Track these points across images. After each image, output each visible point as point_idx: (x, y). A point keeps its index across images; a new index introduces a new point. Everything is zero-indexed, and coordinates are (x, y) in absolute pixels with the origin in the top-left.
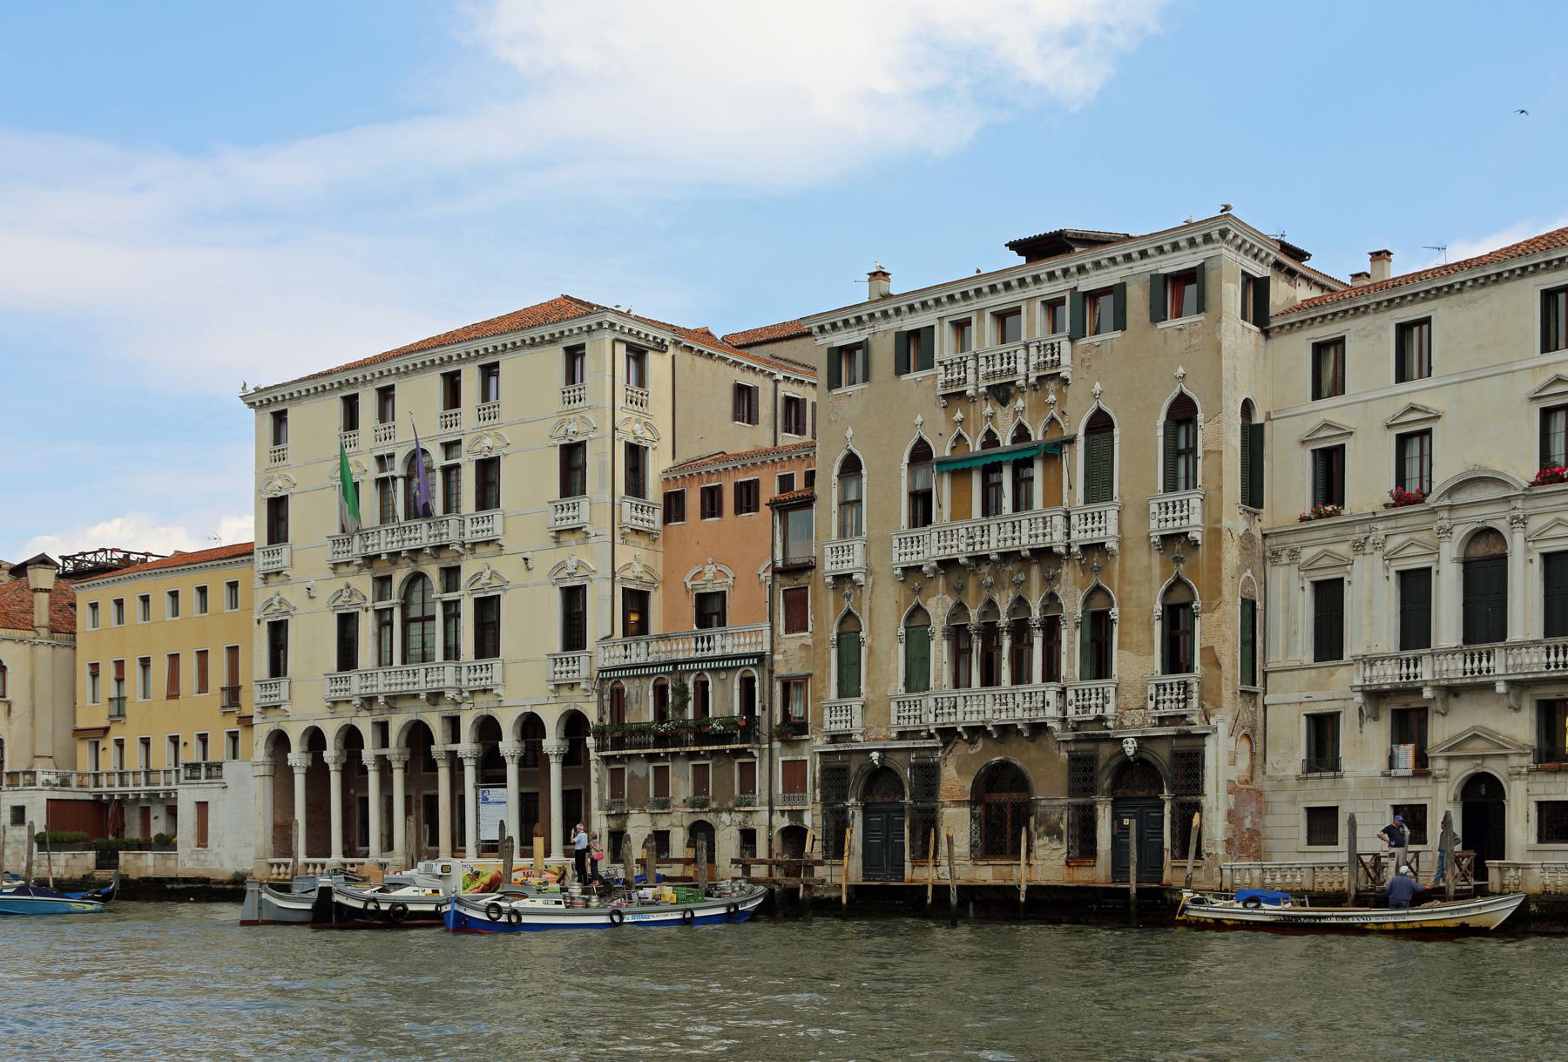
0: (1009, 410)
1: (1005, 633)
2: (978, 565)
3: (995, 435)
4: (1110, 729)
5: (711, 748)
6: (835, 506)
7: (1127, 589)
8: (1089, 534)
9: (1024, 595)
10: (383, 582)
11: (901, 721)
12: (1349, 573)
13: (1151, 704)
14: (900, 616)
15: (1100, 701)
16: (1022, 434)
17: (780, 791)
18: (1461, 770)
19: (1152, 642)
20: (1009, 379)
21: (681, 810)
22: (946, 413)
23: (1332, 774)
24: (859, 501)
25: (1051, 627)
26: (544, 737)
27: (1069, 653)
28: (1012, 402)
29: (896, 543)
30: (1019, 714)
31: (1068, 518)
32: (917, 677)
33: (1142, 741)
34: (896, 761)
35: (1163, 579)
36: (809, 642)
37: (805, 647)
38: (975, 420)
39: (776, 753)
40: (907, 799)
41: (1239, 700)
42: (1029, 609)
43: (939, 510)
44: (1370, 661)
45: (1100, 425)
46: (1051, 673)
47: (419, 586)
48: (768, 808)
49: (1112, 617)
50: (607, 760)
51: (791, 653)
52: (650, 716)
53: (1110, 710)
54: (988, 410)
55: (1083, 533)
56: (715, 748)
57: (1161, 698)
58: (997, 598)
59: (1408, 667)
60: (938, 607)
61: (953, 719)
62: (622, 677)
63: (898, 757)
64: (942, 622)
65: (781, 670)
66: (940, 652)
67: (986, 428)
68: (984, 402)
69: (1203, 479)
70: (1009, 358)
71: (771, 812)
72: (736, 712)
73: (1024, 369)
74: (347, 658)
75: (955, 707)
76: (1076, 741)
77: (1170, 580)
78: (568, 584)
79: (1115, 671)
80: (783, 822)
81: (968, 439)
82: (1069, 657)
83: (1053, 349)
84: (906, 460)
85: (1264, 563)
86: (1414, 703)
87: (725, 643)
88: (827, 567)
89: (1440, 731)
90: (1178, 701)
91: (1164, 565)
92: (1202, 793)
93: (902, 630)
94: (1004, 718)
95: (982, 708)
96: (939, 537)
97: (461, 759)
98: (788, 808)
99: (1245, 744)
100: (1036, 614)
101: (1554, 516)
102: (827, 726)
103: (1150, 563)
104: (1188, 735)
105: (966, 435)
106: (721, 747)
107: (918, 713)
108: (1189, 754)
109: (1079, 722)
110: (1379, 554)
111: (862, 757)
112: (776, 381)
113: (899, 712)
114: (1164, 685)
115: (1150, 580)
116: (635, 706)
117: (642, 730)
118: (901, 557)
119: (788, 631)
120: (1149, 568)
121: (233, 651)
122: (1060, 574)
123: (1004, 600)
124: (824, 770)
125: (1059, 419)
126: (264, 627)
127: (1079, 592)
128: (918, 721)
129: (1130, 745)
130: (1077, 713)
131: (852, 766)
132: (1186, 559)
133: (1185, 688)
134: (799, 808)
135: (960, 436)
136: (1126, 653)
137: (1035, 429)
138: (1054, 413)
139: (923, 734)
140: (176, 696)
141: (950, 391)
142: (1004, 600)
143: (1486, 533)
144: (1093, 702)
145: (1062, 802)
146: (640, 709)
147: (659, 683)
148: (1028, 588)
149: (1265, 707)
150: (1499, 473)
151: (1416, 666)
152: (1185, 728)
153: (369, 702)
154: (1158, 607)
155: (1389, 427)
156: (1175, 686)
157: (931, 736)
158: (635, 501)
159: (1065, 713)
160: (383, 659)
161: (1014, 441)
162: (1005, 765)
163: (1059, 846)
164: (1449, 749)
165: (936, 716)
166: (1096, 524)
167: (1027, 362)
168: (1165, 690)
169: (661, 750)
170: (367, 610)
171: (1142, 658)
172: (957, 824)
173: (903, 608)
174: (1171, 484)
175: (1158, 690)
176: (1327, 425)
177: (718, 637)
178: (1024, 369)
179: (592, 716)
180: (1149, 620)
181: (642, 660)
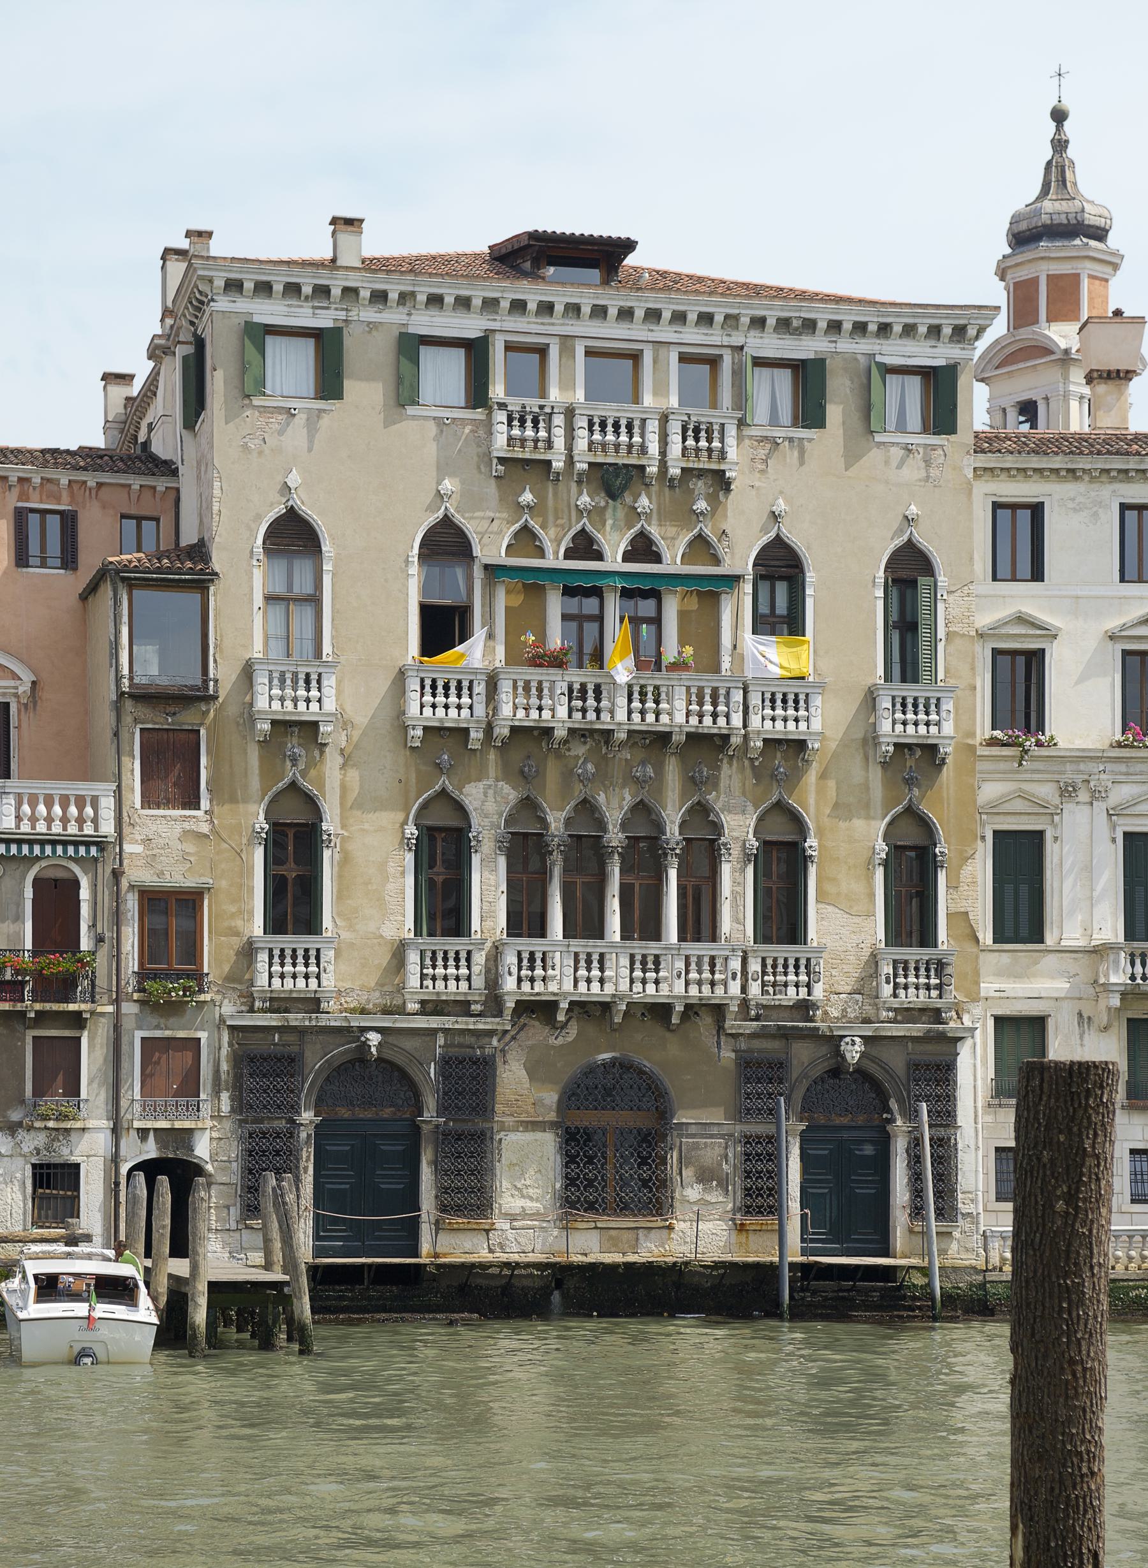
1: (616, 857)
9: (650, 801)
13: (887, 990)
19: (872, 896)
35: (887, 807)
39: (127, 1024)
40: (427, 1116)
49: (809, 852)
53: (818, 992)
54: (585, 500)
57: (901, 980)
63: (409, 1044)
64: (494, 826)
67: (579, 527)
68: (574, 486)
69: (946, 671)
71: (116, 1131)
76: (754, 1036)
77: (899, 808)
82: (735, 906)
90: (928, 987)
91: (888, 784)
95: (464, 971)
98: (163, 1124)
100: (673, 832)
103: (868, 777)
105: (538, 529)
109: (764, 1007)
114: (906, 962)
120: (866, 787)
122: (718, 778)
123: (615, 803)
125: (713, 539)
127: (750, 808)
129: (857, 1048)
131: (308, 1054)
135: (526, 529)
136: (830, 909)
141: (515, 455)
142: (615, 803)
144: (792, 977)
161: (628, 557)
162: (623, 1066)
163: (721, 1199)
168: (905, 969)
171: (856, 920)
173: (413, 794)
176: (1021, 619)
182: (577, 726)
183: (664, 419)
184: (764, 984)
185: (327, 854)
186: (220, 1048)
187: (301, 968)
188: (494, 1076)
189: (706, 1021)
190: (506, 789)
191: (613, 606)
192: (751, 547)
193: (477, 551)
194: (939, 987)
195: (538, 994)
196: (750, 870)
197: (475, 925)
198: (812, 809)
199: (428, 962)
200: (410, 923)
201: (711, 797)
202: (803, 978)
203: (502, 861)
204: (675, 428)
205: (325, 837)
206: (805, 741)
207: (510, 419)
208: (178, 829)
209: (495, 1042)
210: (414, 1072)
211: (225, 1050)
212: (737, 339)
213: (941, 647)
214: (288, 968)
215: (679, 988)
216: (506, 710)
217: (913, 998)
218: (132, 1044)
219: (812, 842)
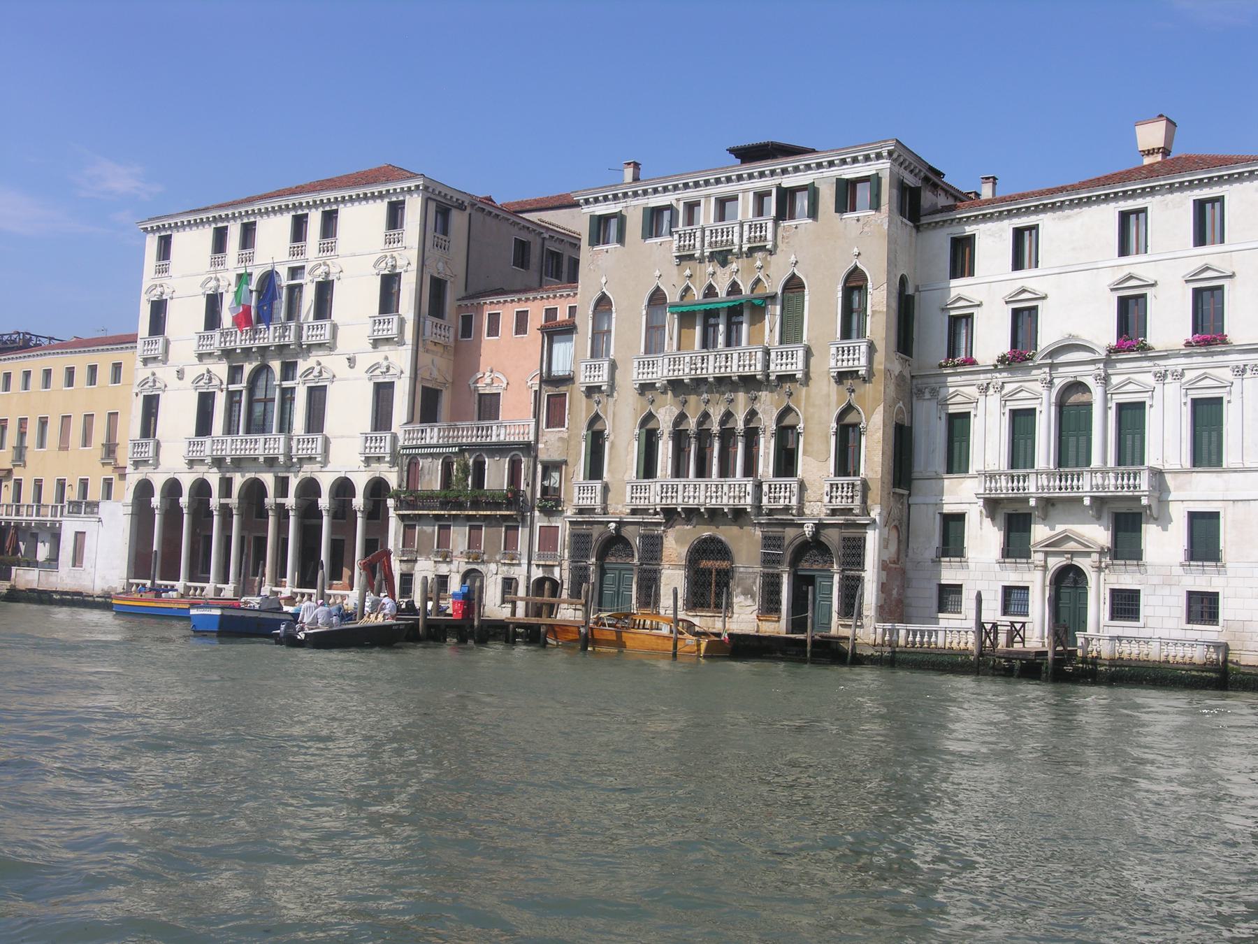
2: (698, 385)
4: (792, 514)
5: (485, 513)
6: (590, 335)
7: (811, 410)
8: (784, 368)
10: (234, 373)
11: (634, 500)
13: (826, 499)
15: (788, 494)
16: (734, 289)
17: (537, 550)
18: (1055, 563)
20: (729, 248)
21: (459, 559)
22: (678, 270)
23: (958, 559)
24: (609, 331)
25: (751, 435)
28: (728, 266)
29: (636, 364)
30: (725, 501)
31: (767, 352)
32: (648, 469)
34: (627, 532)
35: (838, 405)
36: (566, 435)
37: (561, 439)
38: (700, 277)
41: (891, 499)
44: (991, 476)
45: (794, 285)
46: (750, 469)
47: (264, 376)
48: (527, 562)
50: (402, 517)
51: (551, 444)
52: (437, 486)
55: (779, 366)
56: (489, 513)
58: (711, 411)
59: (1019, 482)
60: (665, 417)
61: (674, 501)
62: (418, 454)
63: (630, 528)
64: (668, 427)
65: (543, 456)
66: (665, 449)
70: (728, 232)
71: (529, 564)
73: (738, 239)
74: (204, 427)
75: (677, 492)
78: (381, 380)
79: (799, 472)
80: (537, 573)
83: (761, 227)
84: (646, 302)
85: (912, 398)
86: (1021, 509)
87: (498, 434)
88: (582, 380)
89: (1040, 532)
91: (839, 393)
92: (863, 570)
93: (637, 431)
96: (670, 362)
97: (288, 510)
98: (543, 563)
99: (894, 534)
102: (576, 501)
104: (855, 525)
105: (692, 287)
106: (493, 513)
107: (647, 495)
108: (854, 539)
109: (771, 510)
110: (998, 396)
111: (602, 527)
112: (544, 239)
113: (632, 493)
114: (837, 484)
116: (427, 477)
117: (431, 496)
119: (548, 427)
120: (829, 396)
121: (113, 416)
123: (717, 412)
124: (573, 535)
125: (763, 279)
126: (141, 398)
128: (647, 501)
130: (770, 502)
132: (857, 391)
133: (853, 488)
134: (551, 563)
135: (687, 289)
136: (808, 458)
139: (651, 511)
140: (67, 449)
142: (717, 412)
144: (782, 494)
145: (755, 570)
146: (431, 480)
147: (447, 460)
149: (909, 506)
151: (1024, 482)
152: (852, 518)
153: (218, 462)
154: (834, 425)
156: (845, 486)
157: (656, 513)
158: (436, 320)
159: (761, 502)
160: (230, 429)
161: (729, 294)
162: (712, 540)
164: (1047, 546)
165: (662, 498)
166: (789, 360)
167: (741, 236)
168: (837, 488)
169: (446, 512)
170: (222, 391)
172: (673, 580)
173: (639, 412)
174: (846, 334)
175: (832, 488)
177: (494, 428)
178: (738, 239)
179: (393, 479)
180: (827, 437)
181: (434, 441)
184: (770, 498)
188: (662, 543)
196: (773, 441)
197: (659, 473)
198: (803, 409)
200: (635, 474)
201: (757, 407)
203: (671, 443)
204: (746, 228)
207: (680, 237)
208: (557, 437)
209: (662, 528)
213: (868, 319)
217: (837, 503)
219: (801, 425)
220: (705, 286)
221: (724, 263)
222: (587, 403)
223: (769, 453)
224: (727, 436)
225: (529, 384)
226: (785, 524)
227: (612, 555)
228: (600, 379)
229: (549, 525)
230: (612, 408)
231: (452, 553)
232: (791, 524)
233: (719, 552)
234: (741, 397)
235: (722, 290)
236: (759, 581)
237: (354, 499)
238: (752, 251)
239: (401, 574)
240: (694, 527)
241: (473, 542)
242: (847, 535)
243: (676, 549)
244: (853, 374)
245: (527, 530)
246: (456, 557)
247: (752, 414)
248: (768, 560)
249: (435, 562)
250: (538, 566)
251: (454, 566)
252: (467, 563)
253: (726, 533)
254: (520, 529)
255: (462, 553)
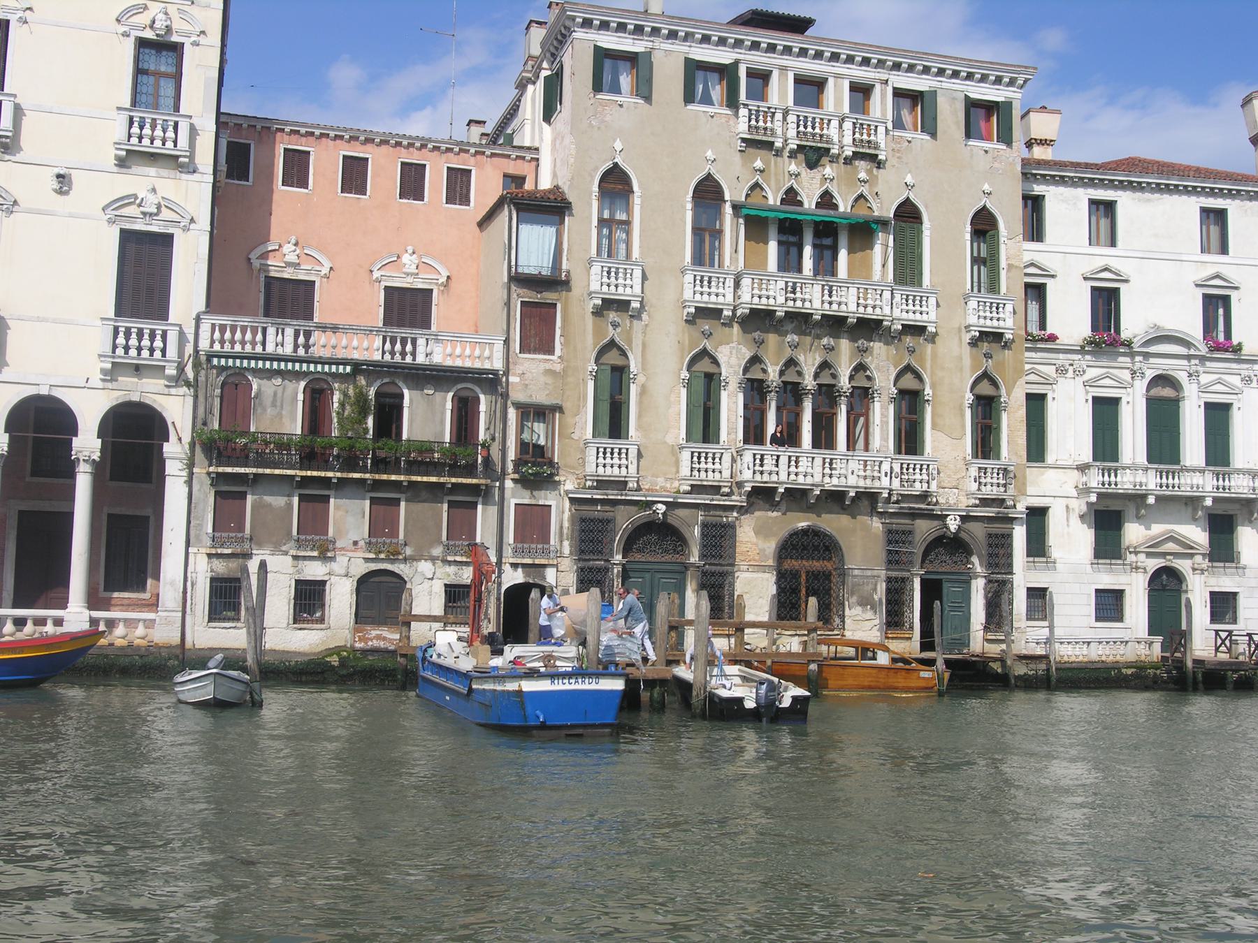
0: (816, 174)
3: (796, 194)
6: (595, 222)
12: (1239, 400)
14: (682, 358)
16: (827, 200)
17: (511, 541)
18: (1154, 564)
19: (963, 426)
21: (350, 554)
22: (742, 157)
23: (1044, 559)
25: (862, 396)
26: (76, 436)
27: (882, 426)
28: (820, 169)
33: (964, 519)
35: (974, 370)
36: (558, 367)
38: (776, 174)
39: (508, 494)
42: (834, 376)
43: (734, 255)
45: (908, 214)
49: (926, 398)
52: (294, 425)
54: (793, 168)
57: (983, 480)
58: (801, 358)
65: (517, 395)
66: (732, 406)
67: (788, 185)
69: (1007, 288)
72: (447, 439)
81: (767, 188)
89: (1133, 533)
90: (998, 485)
91: (973, 358)
92: (1011, 573)
93: (685, 374)
94: (833, 483)
101: (1217, 376)
105: (765, 186)
109: (901, 495)
114: (986, 469)
115: (961, 370)
116: (270, 411)
117: (283, 444)
118: (692, 294)
120: (960, 358)
123: (810, 361)
125: (869, 198)
127: (892, 368)
134: (543, 561)
135: (756, 186)
137: (845, 200)
138: (865, 189)
142: (810, 361)
143: (1162, 380)
144: (918, 477)
145: (875, 573)
146: (280, 416)
148: (838, 355)
150: (1188, 335)
154: (969, 398)
155: (1085, 279)
161: (818, 205)
177: (421, 342)
181: (288, 350)
182: (790, 310)
183: (842, 121)
185: (633, 388)
186: (563, 512)
187: (616, 461)
189: (865, 503)
190: (744, 350)
191: (808, 237)
192: (892, 204)
193: (727, 197)
194: (1005, 486)
195: (766, 482)
196: (891, 408)
197: (723, 436)
198: (929, 371)
199: (695, 459)
202: (925, 477)
203: (741, 397)
205: (631, 376)
206: (926, 327)
210: (684, 530)
211: (567, 515)
212: (885, 77)
213: (1003, 274)
214: (608, 461)
215: (852, 480)
216: (746, 296)
217: (990, 491)
218: (509, 507)
220: (785, 188)
221: (812, 165)
222: (594, 324)
223: (887, 423)
224: (827, 394)
225: (376, 275)
226: (914, 515)
227: (639, 551)
228: (628, 291)
229: (533, 502)
230: (640, 336)
231: (334, 543)
232: (930, 516)
233: (816, 548)
234: (845, 345)
235: (809, 201)
236: (882, 587)
237: (165, 444)
238: (856, 155)
239: (212, 580)
240: (784, 514)
241: (381, 527)
242: (994, 531)
243: (756, 544)
244: (996, 337)
245: (493, 510)
246: (343, 549)
247: (860, 368)
248: (893, 559)
249: (295, 558)
250: (514, 566)
251: (340, 564)
252: (367, 560)
253: (832, 523)
254: (480, 507)
255: (355, 543)
